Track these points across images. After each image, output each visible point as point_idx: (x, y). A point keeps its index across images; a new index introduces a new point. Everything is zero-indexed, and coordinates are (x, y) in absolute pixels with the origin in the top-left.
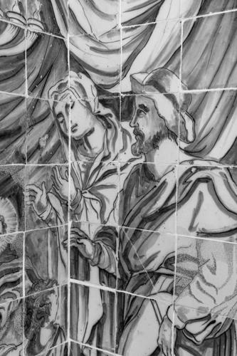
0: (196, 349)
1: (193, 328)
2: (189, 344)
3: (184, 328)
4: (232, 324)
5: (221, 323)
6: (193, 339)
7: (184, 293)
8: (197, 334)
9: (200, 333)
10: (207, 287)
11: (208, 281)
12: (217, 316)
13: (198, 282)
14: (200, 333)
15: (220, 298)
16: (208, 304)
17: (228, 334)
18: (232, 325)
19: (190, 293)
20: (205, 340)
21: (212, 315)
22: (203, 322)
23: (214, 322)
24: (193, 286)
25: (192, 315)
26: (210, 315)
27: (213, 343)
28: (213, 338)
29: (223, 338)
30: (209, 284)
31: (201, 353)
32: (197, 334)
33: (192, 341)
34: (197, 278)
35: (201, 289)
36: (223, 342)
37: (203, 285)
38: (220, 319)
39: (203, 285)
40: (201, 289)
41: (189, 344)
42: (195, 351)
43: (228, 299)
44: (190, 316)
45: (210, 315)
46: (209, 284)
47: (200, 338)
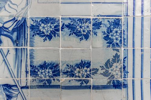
0: (9, 34)
1: (6, 26)
2: (5, 33)
3: (3, 26)
4: (25, 20)
5: (20, 20)
6: (7, 30)
7: (2, 10)
8: (9, 28)
9: (10, 27)
10: (13, 5)
11: (13, 3)
12: (18, 17)
13: (9, 4)
14: (10, 27)
15: (19, 9)
16: (14, 13)
17: (23, 24)
18: (25, 20)
19: (5, 9)
20: (13, 29)
21: (16, 17)
22: (12, 21)
23: (17, 20)
24: (7, 6)
25: (7, 19)
26: (15, 18)
27: (16, 30)
28: (16, 28)
29: (21, 27)
30: (14, 4)
31: (11, 35)
32: (9, 28)
33: (7, 31)
34: (8, 2)
35: (10, 7)
36: (21, 28)
37: (11, 5)
38: (20, 19)
39: (11, 5)
40: (10, 7)
41: (5, 33)
42: (8, 35)
43: (22, 9)
44: (5, 21)
45: (15, 18)
46: (14, 4)
47: (10, 29)
